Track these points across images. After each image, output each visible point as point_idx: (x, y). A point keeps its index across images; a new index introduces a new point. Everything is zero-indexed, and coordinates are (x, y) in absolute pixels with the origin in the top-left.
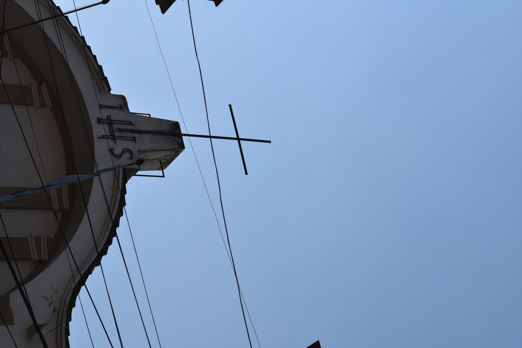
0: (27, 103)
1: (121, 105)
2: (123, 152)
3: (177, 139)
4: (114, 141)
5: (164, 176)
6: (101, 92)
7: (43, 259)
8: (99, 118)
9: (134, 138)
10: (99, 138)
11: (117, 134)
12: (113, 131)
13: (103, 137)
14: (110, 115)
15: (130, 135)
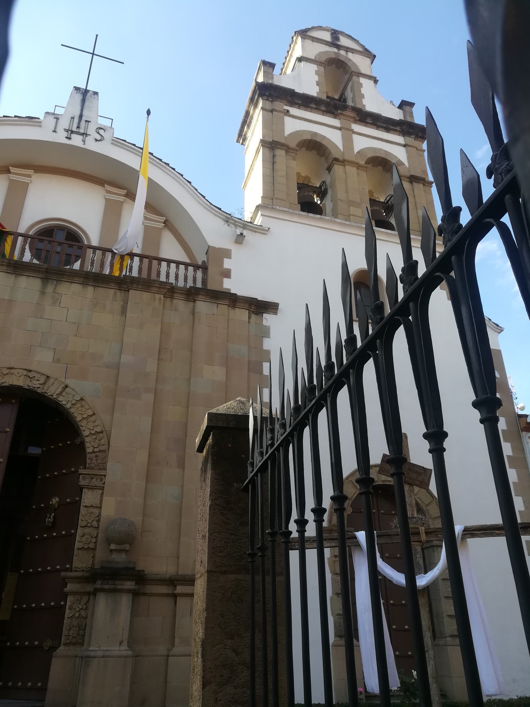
0: (25, 187)
1: (54, 118)
2: (99, 133)
3: (89, 94)
4: (88, 136)
5: (112, 120)
6: (40, 126)
7: (164, 221)
8: (66, 137)
9: (86, 121)
10: (84, 144)
11: (82, 131)
12: (80, 133)
13: (84, 141)
14: (64, 129)
15: (83, 123)
